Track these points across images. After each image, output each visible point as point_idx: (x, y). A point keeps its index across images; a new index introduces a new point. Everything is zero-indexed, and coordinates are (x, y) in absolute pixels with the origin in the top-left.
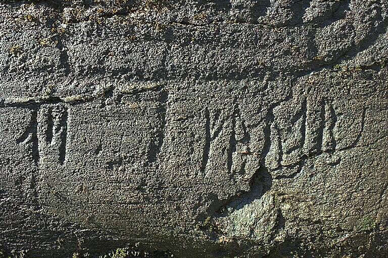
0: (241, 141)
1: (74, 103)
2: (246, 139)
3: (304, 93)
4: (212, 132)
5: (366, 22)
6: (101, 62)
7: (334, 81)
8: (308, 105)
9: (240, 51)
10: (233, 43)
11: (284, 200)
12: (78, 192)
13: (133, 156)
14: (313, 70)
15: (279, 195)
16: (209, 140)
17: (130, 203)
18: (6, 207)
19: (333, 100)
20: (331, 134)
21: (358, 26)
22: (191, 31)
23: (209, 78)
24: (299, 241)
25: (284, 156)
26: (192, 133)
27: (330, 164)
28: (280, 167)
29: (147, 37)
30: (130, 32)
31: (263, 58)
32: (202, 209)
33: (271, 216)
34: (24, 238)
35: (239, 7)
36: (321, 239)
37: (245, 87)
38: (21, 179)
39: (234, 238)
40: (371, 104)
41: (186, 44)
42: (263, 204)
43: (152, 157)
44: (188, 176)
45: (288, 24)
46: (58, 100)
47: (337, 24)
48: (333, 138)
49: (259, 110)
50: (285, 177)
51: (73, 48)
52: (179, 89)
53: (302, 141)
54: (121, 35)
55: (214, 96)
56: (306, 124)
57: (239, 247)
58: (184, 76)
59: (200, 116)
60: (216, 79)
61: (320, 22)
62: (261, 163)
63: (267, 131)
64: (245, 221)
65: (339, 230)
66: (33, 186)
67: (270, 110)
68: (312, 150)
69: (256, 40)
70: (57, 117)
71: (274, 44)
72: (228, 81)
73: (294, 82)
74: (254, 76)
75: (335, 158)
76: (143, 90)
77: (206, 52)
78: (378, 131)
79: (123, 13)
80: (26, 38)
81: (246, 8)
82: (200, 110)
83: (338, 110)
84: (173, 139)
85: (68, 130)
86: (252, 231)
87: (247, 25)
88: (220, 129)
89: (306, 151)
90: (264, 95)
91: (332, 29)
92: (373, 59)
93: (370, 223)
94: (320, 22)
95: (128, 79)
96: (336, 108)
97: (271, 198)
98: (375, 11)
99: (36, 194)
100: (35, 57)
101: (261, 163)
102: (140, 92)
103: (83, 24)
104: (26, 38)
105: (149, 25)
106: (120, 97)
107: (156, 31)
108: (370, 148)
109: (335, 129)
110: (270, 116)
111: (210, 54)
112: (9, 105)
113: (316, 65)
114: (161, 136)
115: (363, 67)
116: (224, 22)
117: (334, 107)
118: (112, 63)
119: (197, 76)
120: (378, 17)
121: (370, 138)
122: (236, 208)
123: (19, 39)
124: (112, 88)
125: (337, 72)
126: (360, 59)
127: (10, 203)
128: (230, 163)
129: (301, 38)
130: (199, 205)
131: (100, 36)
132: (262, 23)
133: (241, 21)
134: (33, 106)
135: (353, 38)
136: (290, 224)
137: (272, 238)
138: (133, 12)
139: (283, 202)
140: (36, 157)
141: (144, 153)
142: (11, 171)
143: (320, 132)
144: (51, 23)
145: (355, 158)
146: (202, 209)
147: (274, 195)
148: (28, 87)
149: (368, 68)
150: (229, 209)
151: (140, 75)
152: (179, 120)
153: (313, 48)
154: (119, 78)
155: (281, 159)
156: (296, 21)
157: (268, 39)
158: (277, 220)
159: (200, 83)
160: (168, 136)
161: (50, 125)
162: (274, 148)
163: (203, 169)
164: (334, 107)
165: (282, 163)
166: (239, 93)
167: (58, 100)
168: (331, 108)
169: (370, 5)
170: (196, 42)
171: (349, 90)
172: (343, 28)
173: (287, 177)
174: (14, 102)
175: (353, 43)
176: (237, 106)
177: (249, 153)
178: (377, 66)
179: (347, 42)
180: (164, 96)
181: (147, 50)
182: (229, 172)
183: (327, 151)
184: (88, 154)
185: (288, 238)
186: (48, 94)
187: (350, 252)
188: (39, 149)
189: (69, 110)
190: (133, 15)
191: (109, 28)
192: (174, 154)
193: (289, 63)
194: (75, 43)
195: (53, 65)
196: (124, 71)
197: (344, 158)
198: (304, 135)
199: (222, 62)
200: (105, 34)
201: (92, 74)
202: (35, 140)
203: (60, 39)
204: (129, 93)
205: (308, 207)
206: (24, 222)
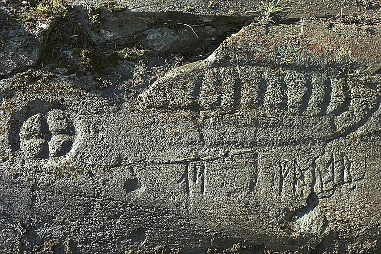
0: (300, 178)
1: (208, 161)
2: (302, 177)
4: (283, 174)
6: (222, 139)
8: (334, 157)
9: (295, 130)
11: (326, 210)
12: (212, 209)
13: (241, 188)
15: (324, 207)
17: (241, 215)
22: (268, 121)
24: (338, 233)
25: (324, 185)
27: (350, 188)
28: (323, 191)
29: (245, 124)
30: (236, 122)
31: (307, 133)
32: (282, 217)
34: (179, 240)
35: (292, 107)
36: (350, 232)
37: (299, 149)
38: (180, 203)
39: (301, 234)
41: (266, 127)
42: (314, 213)
43: (252, 189)
45: (319, 115)
46: (199, 159)
47: (345, 114)
50: (326, 197)
51: (206, 132)
52: (264, 151)
56: (334, 167)
57: (304, 239)
60: (283, 146)
61: (337, 112)
62: (312, 190)
64: (305, 223)
65: (360, 225)
67: (314, 161)
71: (312, 126)
73: (325, 145)
74: (303, 143)
75: (352, 186)
76: (245, 152)
78: (375, 170)
79: (232, 113)
80: (180, 128)
81: (296, 107)
84: (262, 179)
85: (205, 175)
86: (311, 228)
89: (336, 181)
92: (367, 131)
94: (337, 112)
95: (236, 147)
96: (350, 158)
97: (319, 210)
98: (365, 106)
99: (188, 212)
103: (211, 119)
104: (180, 128)
105: (246, 118)
106: (232, 157)
107: (250, 121)
109: (351, 170)
110: (314, 164)
112: (173, 163)
113: (337, 136)
114: (256, 178)
115: (362, 136)
116: (285, 115)
117: (349, 158)
118: (228, 139)
119: (273, 144)
120: (367, 109)
125: (348, 139)
126: (359, 132)
127: (173, 218)
129: (327, 122)
130: (280, 214)
131: (220, 125)
133: (294, 115)
134: (185, 162)
137: (322, 232)
138: (237, 112)
140: (188, 191)
141: (247, 186)
142: (174, 199)
143: (342, 171)
146: (282, 217)
147: (320, 208)
149: (365, 136)
150: (296, 217)
153: (334, 127)
154: (232, 147)
155: (322, 187)
156: (323, 113)
158: (324, 221)
159: (275, 148)
160: (260, 176)
161: (195, 174)
162: (318, 181)
163: (280, 194)
164: (349, 158)
165: (323, 189)
167: (199, 159)
168: (347, 158)
169: (362, 103)
171: (356, 148)
172: (349, 115)
176: (295, 160)
178: (369, 135)
179: (351, 123)
180: (256, 155)
181: (246, 132)
182: (295, 195)
183: (348, 182)
185: (331, 232)
186: (194, 156)
187: (368, 239)
188: (189, 187)
189: (205, 165)
190: (237, 114)
191: (225, 121)
196: (234, 143)
198: (334, 174)
199: (286, 136)
201: (217, 145)
202: (187, 181)
203: (199, 127)
205: (341, 213)
206: (180, 230)
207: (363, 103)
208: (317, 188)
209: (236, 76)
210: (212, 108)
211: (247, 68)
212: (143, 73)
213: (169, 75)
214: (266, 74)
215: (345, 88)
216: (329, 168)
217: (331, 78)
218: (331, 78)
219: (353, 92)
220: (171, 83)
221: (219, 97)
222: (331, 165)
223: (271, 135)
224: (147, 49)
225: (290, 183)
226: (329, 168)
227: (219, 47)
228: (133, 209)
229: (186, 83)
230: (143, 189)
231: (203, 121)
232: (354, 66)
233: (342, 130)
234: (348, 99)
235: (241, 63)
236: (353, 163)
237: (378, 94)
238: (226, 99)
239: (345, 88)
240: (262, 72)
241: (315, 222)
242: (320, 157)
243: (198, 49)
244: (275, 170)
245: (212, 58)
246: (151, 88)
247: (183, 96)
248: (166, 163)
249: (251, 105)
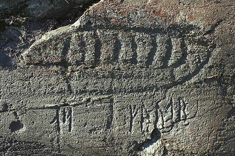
1: (74, 106)
2: (148, 117)
3: (171, 96)
4: (133, 115)
5: (194, 64)
6: (85, 88)
8: (173, 101)
9: (143, 80)
10: (140, 77)
11: (166, 142)
12: (77, 143)
13: (100, 127)
14: (174, 86)
15: (164, 140)
17: (100, 147)
18: (46, 152)
21: (191, 66)
22: (121, 73)
23: (130, 92)
25: (165, 123)
26: (125, 115)
27: (185, 125)
28: (163, 128)
29: (104, 76)
30: (96, 75)
31: (152, 82)
32: (131, 148)
33: (161, 149)
35: (141, 62)
37: (146, 95)
38: (53, 139)
40: (200, 98)
41: (120, 78)
44: (124, 134)
45: (162, 68)
46: (67, 105)
47: (182, 66)
48: (185, 114)
51: (73, 83)
55: (133, 100)
56: (173, 109)
58: (120, 92)
61: (175, 65)
62: (155, 126)
63: (156, 113)
66: (58, 142)
67: (157, 104)
68: (176, 119)
69: (149, 75)
70: (67, 112)
71: (157, 76)
73: (166, 91)
74: (149, 90)
75: (186, 123)
76: (103, 98)
77: (128, 81)
78: (204, 110)
79: (93, 67)
80: (53, 80)
81: (144, 62)
82: (127, 105)
83: (186, 102)
84: (117, 119)
85: (72, 117)
87: (144, 69)
88: (136, 113)
89: (174, 120)
90: (154, 98)
91: (180, 68)
92: (199, 79)
93: (205, 150)
94: (175, 65)
95: (96, 94)
96: (185, 101)
97: (161, 141)
98: (197, 59)
99: (59, 145)
100: (57, 87)
101: (155, 126)
103: (77, 73)
104: (53, 80)
105: (104, 71)
106: (93, 102)
107: (107, 74)
108: (202, 117)
109: (186, 110)
110: (157, 106)
111: (130, 82)
112: (47, 108)
113: (175, 84)
114: (112, 118)
115: (195, 83)
116: (135, 68)
117: (184, 101)
118: (89, 88)
119: (125, 92)
120: (199, 61)
123: (50, 80)
124: (90, 98)
125: (184, 86)
126: (193, 80)
127: (48, 150)
128: (142, 128)
129: (167, 73)
131: (84, 77)
133: (142, 67)
134: (57, 108)
135: (190, 71)
136: (170, 152)
138: (97, 66)
139: (166, 143)
140: (59, 129)
141: (105, 125)
142: (48, 136)
143: (179, 112)
144: (63, 73)
145: (195, 122)
146: (131, 148)
147: (162, 140)
148: (54, 100)
150: (143, 148)
151: (101, 92)
153: (173, 77)
154: (93, 94)
155: (163, 124)
156: (165, 66)
157: (154, 74)
158: (164, 151)
159: (126, 94)
160: (115, 117)
162: (160, 119)
163: (130, 131)
164: (184, 101)
165: (164, 126)
166: (143, 98)
167: (67, 105)
169: (195, 57)
171: (190, 93)
172: (185, 67)
173: (167, 132)
174: (49, 106)
175: (190, 73)
177: (149, 122)
179: (187, 73)
180: (112, 101)
182: (142, 131)
183: (183, 120)
184: (81, 127)
186: (63, 102)
188: (60, 126)
189: (72, 109)
190: (97, 68)
191: (87, 74)
192: (118, 125)
193: (163, 84)
195: (65, 90)
196: (94, 91)
199: (135, 85)
200: (86, 76)
201: (81, 93)
202: (58, 122)
203: (67, 80)
204: (97, 100)
205: (177, 144)
207: (197, 57)
209: (96, 38)
210: (78, 63)
211: (105, 31)
212: (24, 36)
213: (44, 38)
214: (120, 35)
215: (183, 46)
217: (172, 38)
218: (172, 38)
219: (189, 48)
220: (45, 45)
221: (83, 55)
222: (171, 107)
224: (29, 16)
225: (138, 122)
227: (83, 15)
228: (17, 144)
229: (57, 44)
230: (24, 129)
231: (70, 74)
232: (191, 27)
233: (180, 79)
234: (184, 55)
235: (101, 27)
236: (188, 104)
237: (208, 50)
238: (89, 56)
239: (183, 46)
240: (117, 35)
241: (157, 151)
243: (69, 15)
245: (77, 24)
246: (29, 49)
247: (55, 55)
248: (41, 108)
249: (108, 61)
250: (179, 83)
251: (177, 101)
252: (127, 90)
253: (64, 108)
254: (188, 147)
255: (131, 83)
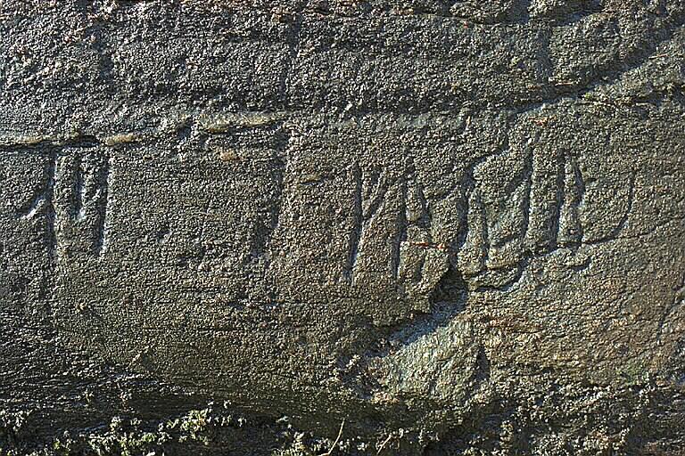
1: (119, 147)
2: (424, 221)
3: (530, 141)
4: (366, 206)
6: (172, 76)
7: (583, 120)
8: (536, 162)
10: (402, 47)
11: (489, 328)
13: (224, 245)
14: (545, 100)
16: (360, 219)
19: (579, 155)
20: (576, 215)
21: (626, 26)
22: (333, 25)
23: (364, 110)
24: (514, 402)
27: (572, 267)
29: (255, 34)
31: (456, 78)
33: (466, 356)
34: (25, 389)
36: (555, 399)
37: (427, 128)
39: (402, 396)
40: (645, 164)
42: (454, 334)
43: (258, 246)
44: (321, 282)
45: (505, 19)
47: (591, 20)
48: (579, 223)
49: (449, 170)
50: (493, 288)
51: (123, 49)
53: (525, 223)
54: (208, 30)
55: (370, 143)
57: (405, 412)
58: (317, 107)
59: (345, 178)
62: (452, 261)
63: (463, 204)
64: (421, 364)
65: (585, 384)
66: (42, 295)
68: (541, 241)
69: (449, 44)
70: (91, 172)
72: (396, 116)
73: (512, 118)
75: (580, 258)
76: (245, 128)
77: (358, 63)
82: (346, 165)
83: (589, 173)
84: (296, 218)
86: (433, 384)
87: (432, 17)
88: (380, 199)
90: (458, 143)
91: (579, 31)
93: (640, 374)
95: (218, 107)
96: (585, 169)
100: (54, 63)
101: (452, 261)
102: (239, 131)
106: (203, 137)
109: (582, 206)
110: (468, 180)
111: (365, 67)
113: (554, 94)
114: (276, 210)
116: (393, 12)
121: (642, 223)
122: (404, 341)
123: (25, 30)
124: (190, 122)
126: (625, 85)
128: (397, 263)
130: (340, 334)
131: (171, 28)
132: (459, 15)
134: (47, 150)
135: (617, 46)
136: (499, 372)
137: (468, 396)
139: (487, 332)
140: (50, 241)
147: (471, 321)
148: (39, 117)
149: (641, 100)
151: (240, 100)
152: (308, 182)
155: (486, 257)
157: (468, 43)
160: (288, 210)
161: (79, 185)
162: (472, 239)
163: (348, 269)
166: (416, 139)
168: (576, 170)
170: (340, 45)
171: (608, 138)
173: (498, 289)
174: (15, 142)
175: (617, 56)
176: (411, 161)
177: (430, 244)
178: (656, 98)
179: (606, 53)
180: (281, 141)
181: (255, 58)
183: (566, 245)
184: (145, 240)
185: (496, 399)
187: (605, 425)
193: (503, 88)
194: (126, 42)
195: (85, 78)
197: (597, 257)
198: (526, 214)
199: (388, 83)
200: (181, 25)
202: (48, 211)
204: (220, 133)
206: (24, 361)
208: (467, 260)
216: (515, 198)
222: (522, 187)
223: (339, 73)
226: (515, 198)
233: (572, 76)
236: (594, 184)
241: (450, 364)
242: (489, 159)
244: (338, 192)
250: (565, 91)
251: (553, 164)
252: (352, 98)
253: (78, 158)
254: (576, 357)
255: (369, 73)
